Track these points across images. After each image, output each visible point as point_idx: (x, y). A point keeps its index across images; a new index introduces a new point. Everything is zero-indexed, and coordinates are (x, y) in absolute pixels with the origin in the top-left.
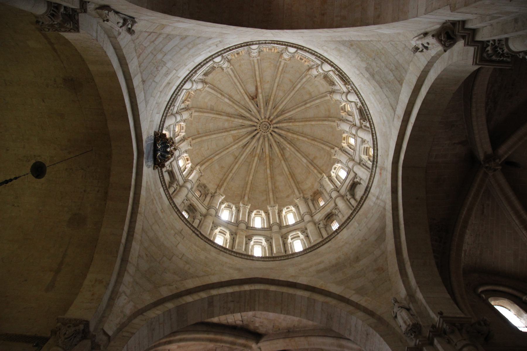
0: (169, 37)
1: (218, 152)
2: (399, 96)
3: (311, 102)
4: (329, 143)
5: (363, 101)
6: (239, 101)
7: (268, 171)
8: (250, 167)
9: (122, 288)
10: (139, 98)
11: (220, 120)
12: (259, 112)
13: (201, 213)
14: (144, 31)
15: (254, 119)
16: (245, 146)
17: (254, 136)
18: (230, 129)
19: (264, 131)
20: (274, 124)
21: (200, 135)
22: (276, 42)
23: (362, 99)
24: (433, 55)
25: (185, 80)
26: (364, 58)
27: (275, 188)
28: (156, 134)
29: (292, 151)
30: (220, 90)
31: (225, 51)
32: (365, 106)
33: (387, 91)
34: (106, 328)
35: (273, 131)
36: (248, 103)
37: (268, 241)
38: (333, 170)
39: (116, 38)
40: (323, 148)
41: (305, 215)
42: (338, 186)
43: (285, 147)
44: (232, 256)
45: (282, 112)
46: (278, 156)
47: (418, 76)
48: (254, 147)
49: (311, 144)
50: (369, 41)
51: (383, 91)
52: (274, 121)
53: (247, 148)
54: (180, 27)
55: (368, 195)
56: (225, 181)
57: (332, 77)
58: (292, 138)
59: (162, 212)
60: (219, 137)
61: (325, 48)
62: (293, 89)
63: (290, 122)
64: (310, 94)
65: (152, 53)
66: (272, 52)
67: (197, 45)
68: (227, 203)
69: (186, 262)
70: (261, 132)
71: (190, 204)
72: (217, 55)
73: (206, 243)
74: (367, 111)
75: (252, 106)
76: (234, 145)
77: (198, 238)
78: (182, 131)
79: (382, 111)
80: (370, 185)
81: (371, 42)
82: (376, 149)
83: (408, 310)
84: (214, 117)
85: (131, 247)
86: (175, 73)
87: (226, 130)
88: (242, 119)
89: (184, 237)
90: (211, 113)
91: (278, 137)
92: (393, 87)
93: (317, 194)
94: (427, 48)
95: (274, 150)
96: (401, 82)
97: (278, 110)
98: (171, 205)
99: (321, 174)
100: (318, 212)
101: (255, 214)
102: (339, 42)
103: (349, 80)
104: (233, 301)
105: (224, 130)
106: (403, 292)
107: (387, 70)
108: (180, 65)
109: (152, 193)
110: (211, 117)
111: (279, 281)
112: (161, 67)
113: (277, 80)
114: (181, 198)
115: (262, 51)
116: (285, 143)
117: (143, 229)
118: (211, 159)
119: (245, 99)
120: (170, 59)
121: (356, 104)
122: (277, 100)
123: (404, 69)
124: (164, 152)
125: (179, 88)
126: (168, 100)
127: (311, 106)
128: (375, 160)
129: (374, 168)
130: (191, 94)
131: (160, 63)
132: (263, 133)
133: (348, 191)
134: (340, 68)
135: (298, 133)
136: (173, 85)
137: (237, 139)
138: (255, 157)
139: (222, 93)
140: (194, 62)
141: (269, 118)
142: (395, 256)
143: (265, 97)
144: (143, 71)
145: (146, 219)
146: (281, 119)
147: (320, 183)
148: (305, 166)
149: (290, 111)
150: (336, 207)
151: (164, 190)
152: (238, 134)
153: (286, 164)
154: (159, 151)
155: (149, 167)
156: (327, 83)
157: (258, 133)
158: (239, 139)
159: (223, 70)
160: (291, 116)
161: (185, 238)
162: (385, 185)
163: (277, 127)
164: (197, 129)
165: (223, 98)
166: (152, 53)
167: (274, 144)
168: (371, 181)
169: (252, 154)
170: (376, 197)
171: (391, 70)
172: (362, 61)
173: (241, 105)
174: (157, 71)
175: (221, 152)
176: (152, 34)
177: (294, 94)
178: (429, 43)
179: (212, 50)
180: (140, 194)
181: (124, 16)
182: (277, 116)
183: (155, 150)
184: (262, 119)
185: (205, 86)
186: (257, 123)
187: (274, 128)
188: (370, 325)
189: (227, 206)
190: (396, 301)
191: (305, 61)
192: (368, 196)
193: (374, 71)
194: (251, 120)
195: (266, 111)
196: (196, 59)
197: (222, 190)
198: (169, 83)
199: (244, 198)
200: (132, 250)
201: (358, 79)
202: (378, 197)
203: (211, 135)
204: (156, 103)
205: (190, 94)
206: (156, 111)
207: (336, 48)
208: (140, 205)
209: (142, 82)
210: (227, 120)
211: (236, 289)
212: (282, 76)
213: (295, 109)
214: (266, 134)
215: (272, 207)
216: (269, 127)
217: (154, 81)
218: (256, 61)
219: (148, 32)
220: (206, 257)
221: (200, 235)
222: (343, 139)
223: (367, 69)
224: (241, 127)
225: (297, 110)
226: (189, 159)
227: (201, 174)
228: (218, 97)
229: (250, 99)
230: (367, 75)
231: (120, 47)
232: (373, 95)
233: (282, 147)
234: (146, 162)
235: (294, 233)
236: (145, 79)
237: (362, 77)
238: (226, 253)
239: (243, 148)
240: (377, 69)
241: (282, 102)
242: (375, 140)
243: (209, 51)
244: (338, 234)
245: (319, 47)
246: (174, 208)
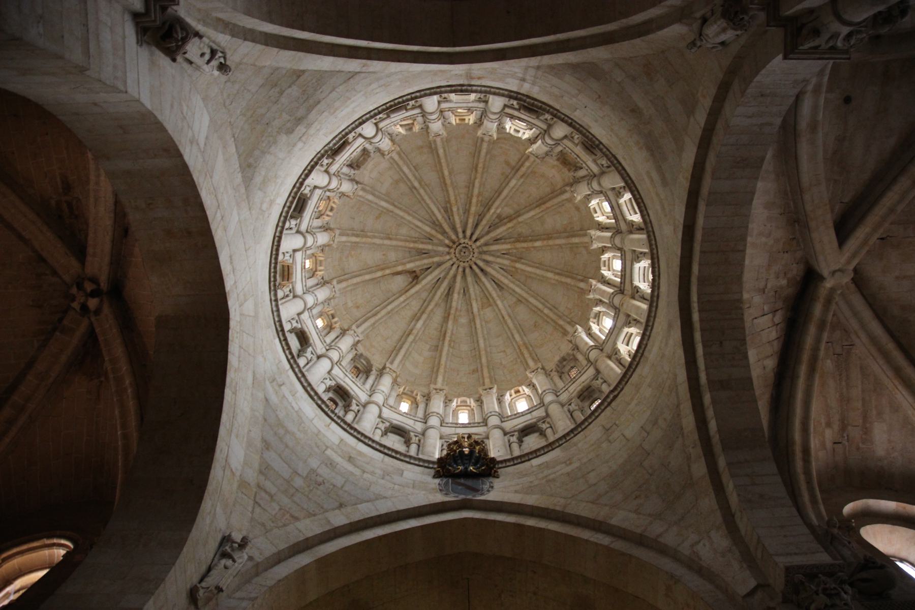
0: (265, 470)
1: (510, 335)
2: (326, 71)
3: (409, 180)
4: (477, 142)
5: (357, 123)
6: (422, 302)
7: (538, 244)
8: (533, 276)
9: (685, 550)
10: (367, 513)
11: (454, 332)
12: (439, 265)
13: (592, 377)
14: (251, 515)
15: (452, 272)
16: (499, 286)
17: (482, 270)
18: (470, 314)
19: (472, 253)
20: (458, 237)
21: (479, 370)
22: (272, 283)
23: (353, 125)
24: (228, 37)
25: (348, 429)
26: (269, 142)
27: (565, 231)
28: (437, 475)
29: (500, 204)
30: (402, 337)
31: (295, 366)
32: (364, 118)
33: (321, 92)
34: (742, 590)
35: (471, 238)
36: (423, 287)
37: (638, 257)
38: (520, 135)
39: (257, 565)
40: (487, 153)
41: (592, 188)
42: (538, 132)
43: (495, 216)
44: (652, 334)
45: (437, 225)
46: (513, 227)
47: (276, 50)
48: (501, 270)
49: (483, 173)
50: (235, 140)
51: (324, 99)
52: (454, 237)
53: (502, 282)
54: (245, 457)
55: (523, 95)
56: (556, 323)
57: (345, 162)
58: (479, 205)
59: (570, 464)
60: (483, 333)
61: (265, 206)
62: (392, 212)
63: (451, 210)
64: (397, 182)
65: (292, 495)
66: (325, 260)
67: (279, 420)
68: (591, 320)
69: (654, 425)
70: (473, 259)
71: (579, 398)
72: (302, 379)
73: (630, 382)
74: (372, 113)
75: (429, 278)
76: (497, 305)
77: (620, 396)
78: (468, 403)
79: (362, 93)
80: (506, 93)
81: (236, 136)
82: (438, 90)
83: (704, 20)
84: (450, 345)
85: (619, 528)
86: (333, 449)
87: (472, 320)
88: (453, 293)
89: (615, 424)
90: (441, 352)
91: (480, 228)
92: (313, 84)
93: (566, 160)
94: (213, 53)
95: (503, 235)
96: (299, 74)
97: (433, 232)
98: (562, 444)
99: (528, 157)
100: (586, 164)
101: (609, 270)
102: (247, 188)
103: (322, 152)
104: (721, 343)
105: (473, 324)
106: (677, 29)
107: (284, 100)
108: (316, 443)
109: (536, 483)
110: (448, 350)
111: (683, 257)
112: (318, 477)
113: (378, 241)
114: (560, 420)
115: (323, 278)
116: (488, 217)
117: (592, 503)
118: (519, 347)
119: (416, 292)
120: (305, 462)
121: (382, 120)
122: (417, 235)
123: (272, 74)
124: (470, 460)
125: (362, 438)
126: (382, 455)
127: (416, 178)
128: (459, 88)
129: (474, 88)
130: (406, 390)
131: (311, 479)
132: (476, 255)
133: (537, 118)
134: (304, 170)
135: (469, 195)
136: (355, 449)
137: (488, 299)
138: (515, 268)
139: (406, 333)
140: (313, 419)
141: (448, 246)
142: (616, 45)
143: (411, 257)
144: (322, 508)
145: (576, 495)
146: (449, 226)
147: (543, 158)
148: (522, 180)
149: (433, 212)
150: (569, 137)
151: (537, 457)
152: (479, 299)
153: (523, 214)
154: (466, 468)
155: (492, 487)
156: (367, 160)
157: (476, 264)
158: (487, 297)
159: (358, 342)
160: (442, 210)
161: (617, 422)
162: (496, 70)
163: (464, 232)
164: (469, 373)
165: (415, 332)
166: (292, 495)
167: (493, 235)
168: (497, 91)
169: (510, 272)
170: (522, 82)
171: (281, 93)
172: (275, 142)
173: (428, 296)
174: (324, 483)
175: (509, 328)
176: (257, 500)
177: (400, 209)
178: (200, 54)
179: (290, 392)
180: (532, 507)
181: (217, 556)
182: (444, 233)
183: (466, 475)
184: (451, 259)
185: (388, 370)
186: (458, 267)
187: (465, 237)
188: (743, 93)
189: (595, 321)
190: (693, 44)
191: (334, 202)
192: (526, 93)
193: (289, 121)
194: (455, 277)
195: (437, 254)
196: (307, 417)
197: (569, 328)
198: (350, 459)
199: (582, 289)
200: (625, 525)
201: (313, 141)
202: (521, 80)
203: (479, 349)
204: (383, 479)
205: (405, 391)
206: (397, 479)
207: (260, 189)
208: (551, 507)
209: (342, 509)
210: (456, 320)
211: (698, 336)
212: (369, 234)
213: (427, 205)
214: (476, 251)
215: (592, 242)
216: (464, 245)
217: (342, 487)
218: (344, 285)
219: (254, 508)
220: (649, 386)
221: (616, 393)
222: (463, 122)
223: (290, 131)
224: (467, 296)
225: (428, 201)
226: (516, 388)
227: (539, 370)
228: (414, 340)
229: (417, 283)
230: (301, 129)
232: (338, 112)
233: (497, 220)
234: (482, 494)
235: (625, 209)
236: (337, 504)
237: (306, 136)
238: (647, 344)
239: (503, 288)
240: (285, 116)
241: (417, 226)
242: (423, 93)
243: (293, 396)
244: (601, 143)
245: (266, 215)
246: (568, 438)
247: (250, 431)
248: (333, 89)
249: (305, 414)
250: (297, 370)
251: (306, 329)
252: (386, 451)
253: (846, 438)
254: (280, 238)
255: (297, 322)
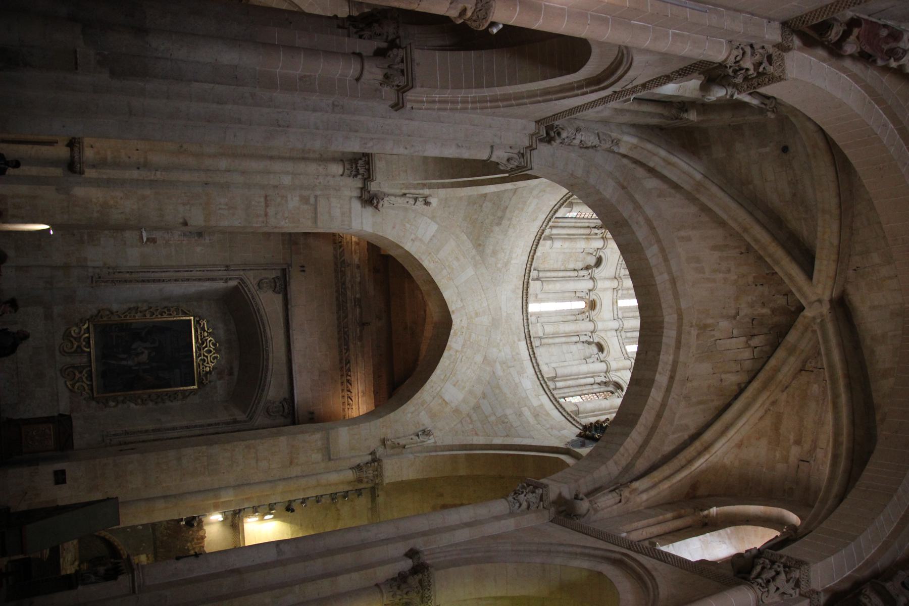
0: (477, 408)
24: (428, 190)
31: (533, 359)
72: (536, 367)
86: (529, 408)
134: (533, 243)
166: (485, 424)
174: (507, 422)
176: (463, 421)
204: (546, 430)
207: (491, 256)
217: (516, 427)
223: (499, 224)
230: (505, 222)
231: (448, 445)
236: (506, 434)
247: (473, 386)
248: (510, 199)
249: (522, 385)
250: (534, 361)
251: (603, 343)
252: (569, 418)
253: (814, 458)
254: (528, 283)
255: (590, 337)
